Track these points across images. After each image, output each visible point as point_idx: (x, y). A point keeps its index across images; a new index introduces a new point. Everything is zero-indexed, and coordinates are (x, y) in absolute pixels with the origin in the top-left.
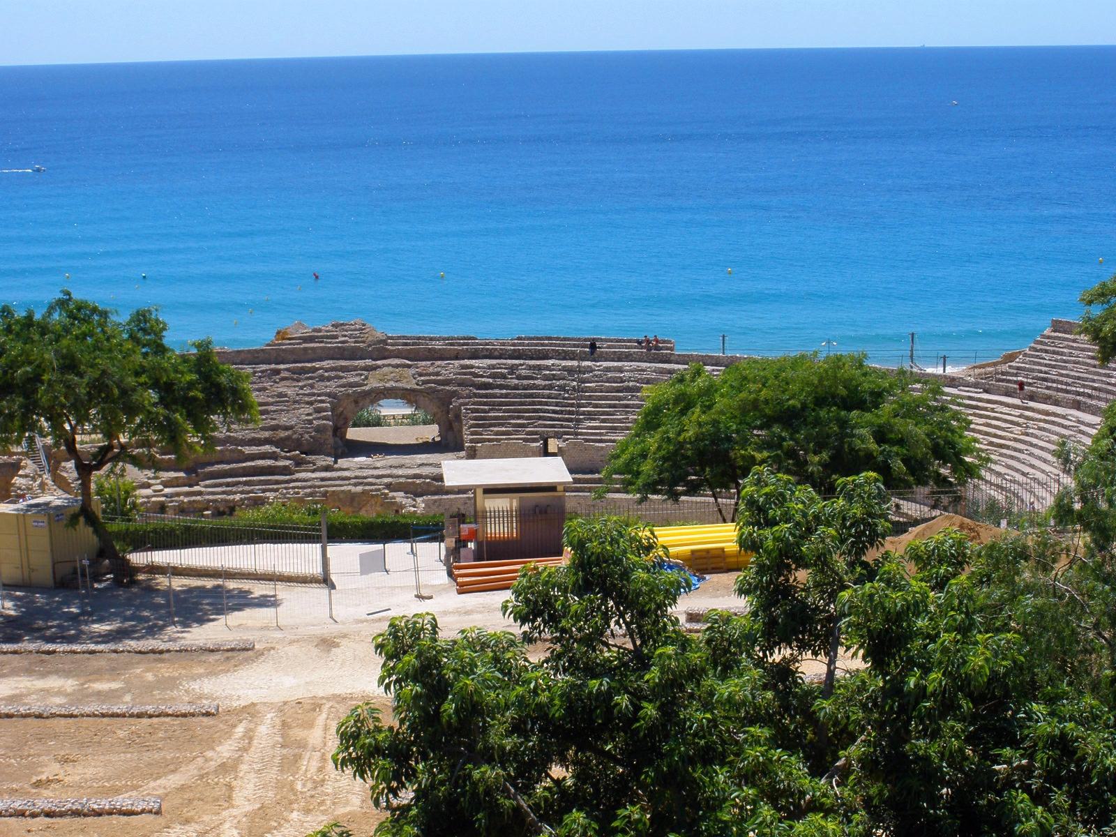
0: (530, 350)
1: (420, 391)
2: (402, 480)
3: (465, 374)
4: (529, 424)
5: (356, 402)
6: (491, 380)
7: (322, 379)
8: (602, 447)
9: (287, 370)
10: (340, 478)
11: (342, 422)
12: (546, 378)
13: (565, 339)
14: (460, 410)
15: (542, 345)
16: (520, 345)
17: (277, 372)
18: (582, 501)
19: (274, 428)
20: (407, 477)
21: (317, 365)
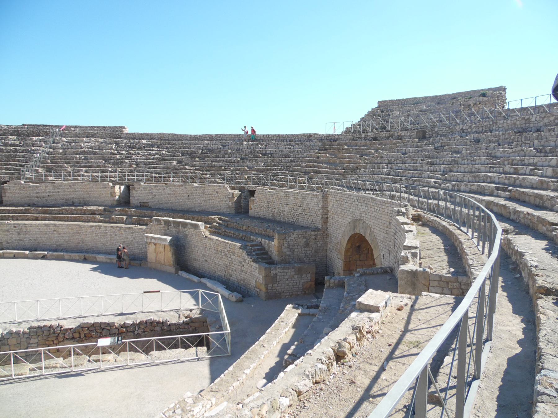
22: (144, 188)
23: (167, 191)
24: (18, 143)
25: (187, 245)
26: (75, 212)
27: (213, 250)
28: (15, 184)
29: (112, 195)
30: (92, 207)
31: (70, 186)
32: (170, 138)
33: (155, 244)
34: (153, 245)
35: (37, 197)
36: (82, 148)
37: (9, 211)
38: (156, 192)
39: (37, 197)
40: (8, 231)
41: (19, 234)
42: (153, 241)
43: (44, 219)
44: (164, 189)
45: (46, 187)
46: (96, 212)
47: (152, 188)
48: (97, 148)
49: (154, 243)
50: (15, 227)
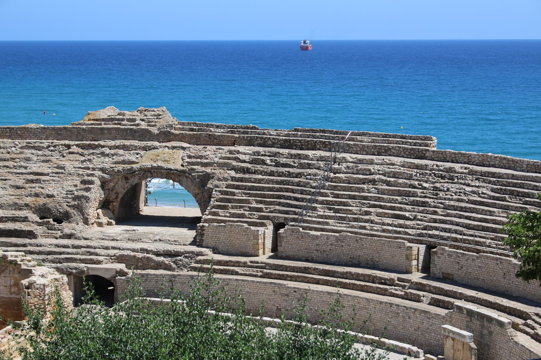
0: (300, 141)
1: (183, 172)
2: (126, 253)
3: (229, 158)
4: (266, 208)
5: (127, 179)
6: (249, 166)
7: (103, 154)
8: (317, 237)
9: (77, 145)
10: (74, 247)
11: (114, 197)
12: (302, 166)
13: (337, 133)
14: (212, 191)
15: (314, 137)
16: (294, 135)
17: (69, 147)
18: (277, 289)
19: (37, 195)
20: (134, 250)
21: (102, 143)
22: (448, 255)
23: (478, 263)
24: (290, 161)
25: (492, 344)
26: (362, 278)
27: (518, 357)
28: (293, 232)
29: (407, 258)
30: (383, 273)
31: (357, 240)
32: (497, 163)
33: (453, 339)
34: (451, 339)
35: (316, 250)
36: (370, 174)
37: (286, 268)
38: (463, 262)
39: (316, 250)
40: (287, 295)
41: (299, 300)
42: (451, 335)
43: (326, 283)
44: (474, 260)
45: (327, 238)
46: (388, 282)
47: (459, 257)
48: (391, 175)
49: (452, 338)
50: (295, 292)
